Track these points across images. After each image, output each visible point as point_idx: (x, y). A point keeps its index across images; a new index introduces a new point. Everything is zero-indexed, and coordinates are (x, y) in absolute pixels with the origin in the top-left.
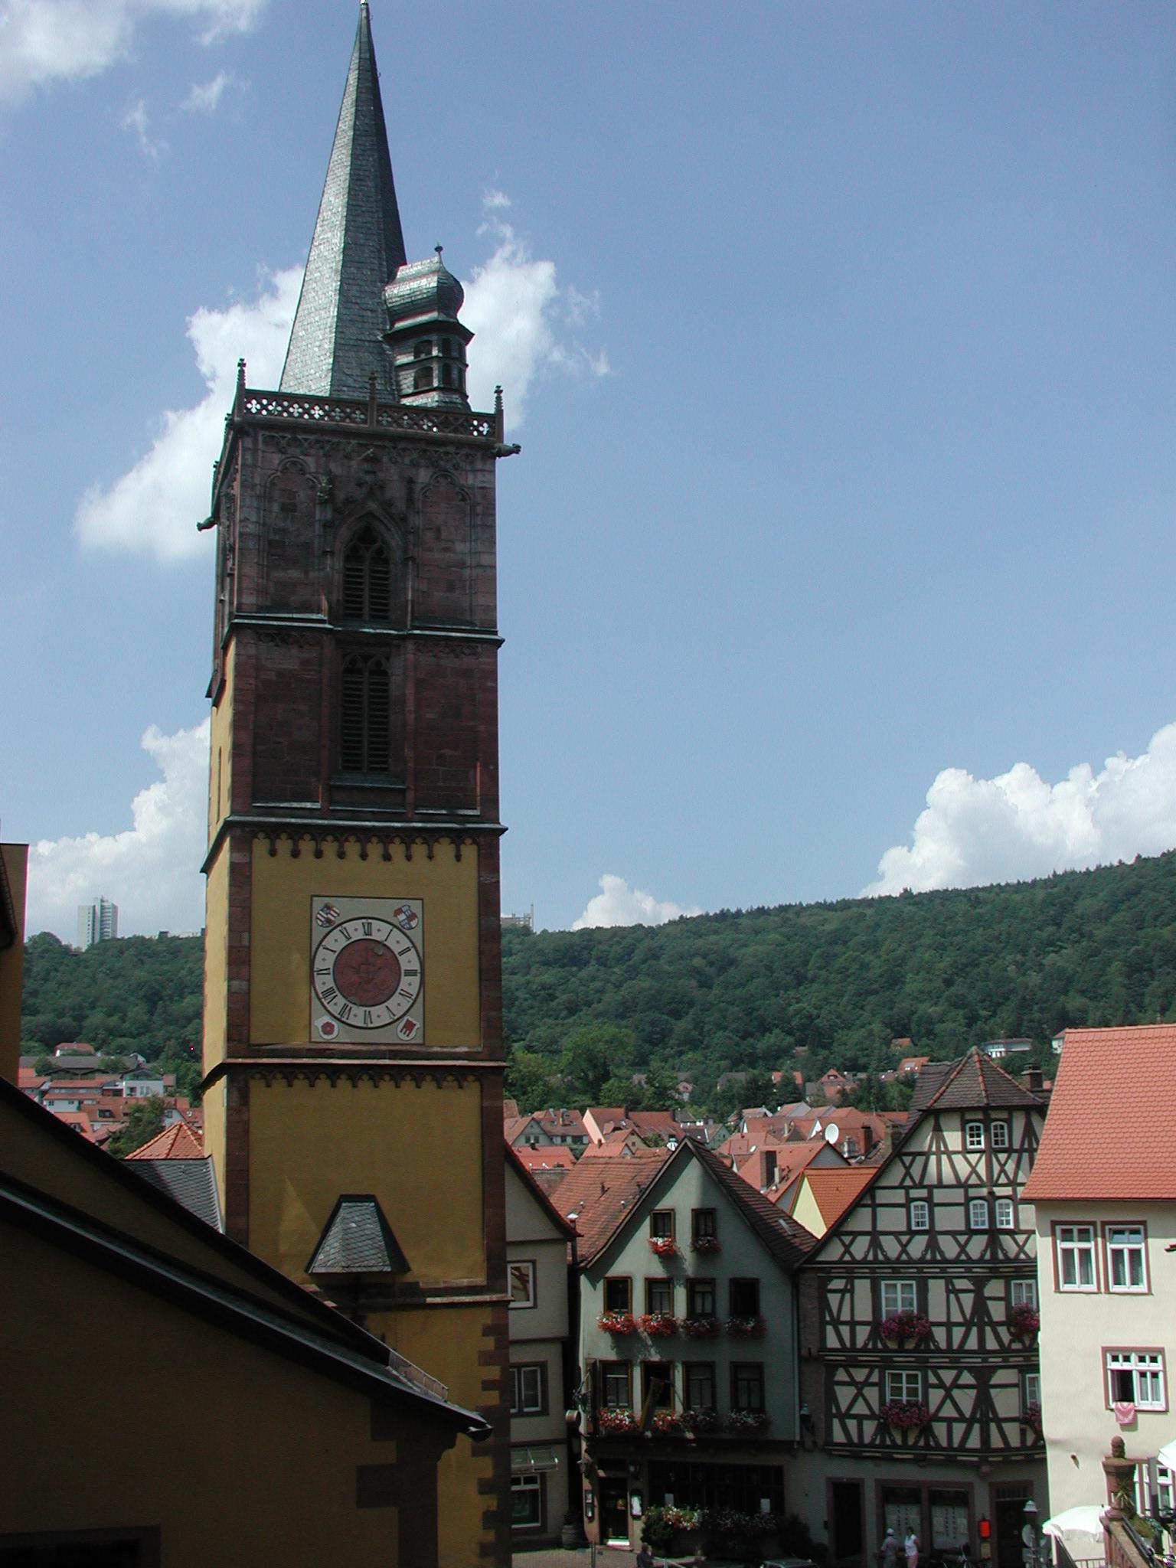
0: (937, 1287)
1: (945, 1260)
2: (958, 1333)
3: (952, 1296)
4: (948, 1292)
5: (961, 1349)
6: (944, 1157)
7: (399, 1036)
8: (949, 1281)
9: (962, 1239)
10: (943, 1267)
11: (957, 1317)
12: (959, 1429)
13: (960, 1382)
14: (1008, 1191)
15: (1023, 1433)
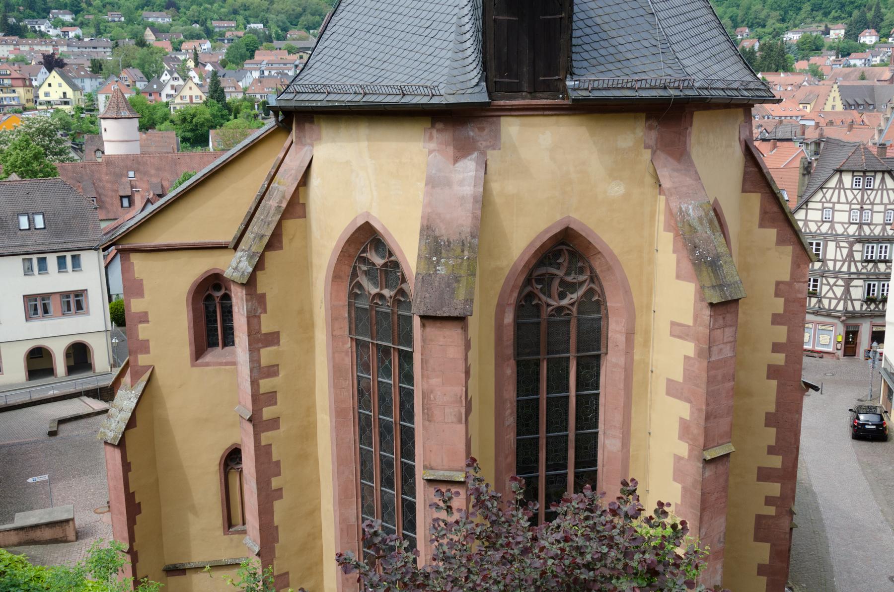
0: (831, 245)
1: (837, 234)
2: (839, 264)
3: (838, 249)
4: (836, 247)
6: (842, 191)
8: (838, 243)
9: (846, 226)
10: (836, 237)
11: (839, 257)
12: (834, 302)
13: (837, 284)
14: (870, 207)
15: (862, 305)
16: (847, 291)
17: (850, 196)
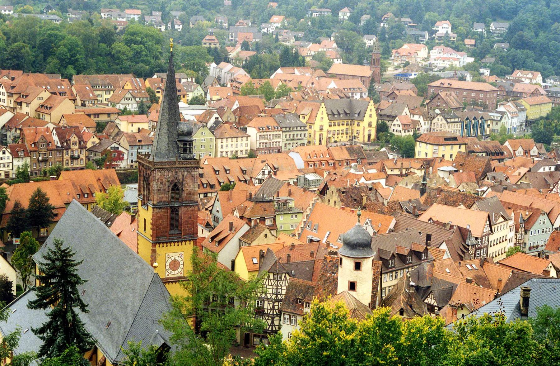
0: (266, 303)
2: (269, 311)
5: (269, 314)
7: (179, 275)
8: (268, 302)
10: (268, 299)
14: (280, 287)
16: (273, 322)
17: (273, 283)
